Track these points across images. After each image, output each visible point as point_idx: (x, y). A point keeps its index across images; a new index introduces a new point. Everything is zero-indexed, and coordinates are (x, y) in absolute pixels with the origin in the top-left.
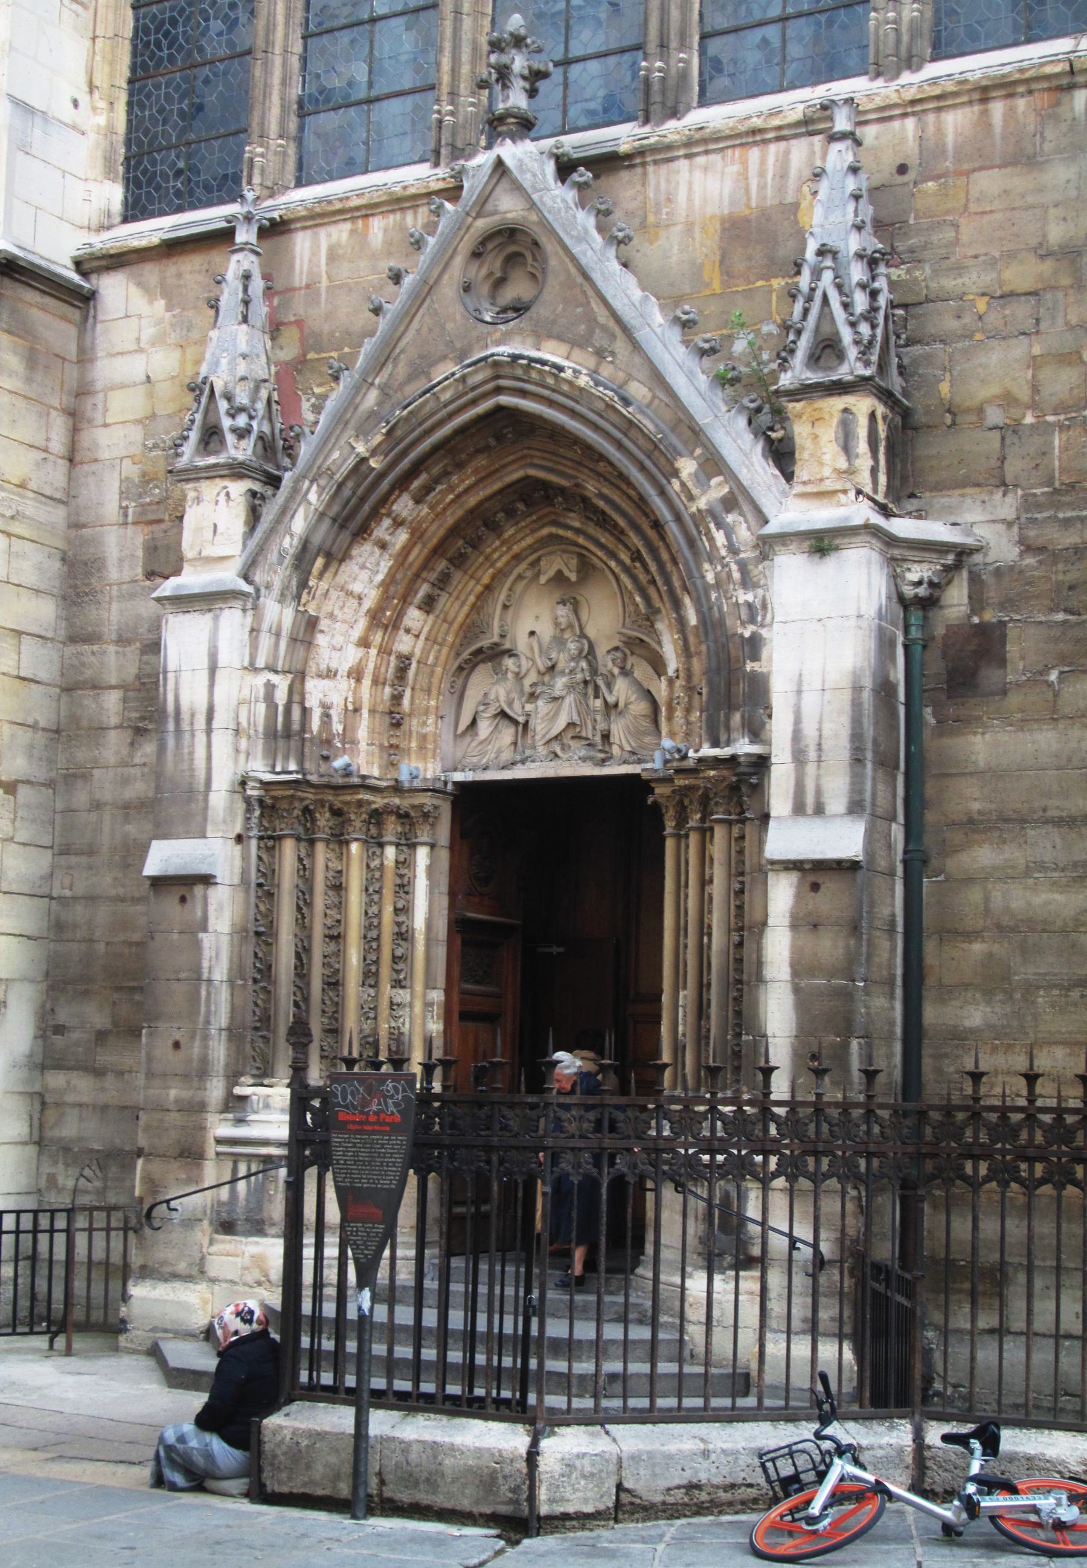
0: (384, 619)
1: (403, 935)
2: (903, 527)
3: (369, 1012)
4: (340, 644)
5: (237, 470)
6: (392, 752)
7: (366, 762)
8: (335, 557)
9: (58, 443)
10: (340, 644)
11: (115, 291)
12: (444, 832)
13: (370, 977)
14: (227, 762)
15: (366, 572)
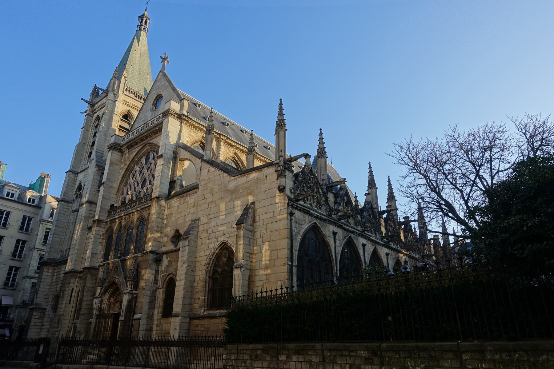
0: (109, 299)
1: (108, 327)
2: (133, 292)
3: (103, 334)
4: (105, 301)
5: (100, 286)
6: (109, 311)
7: (106, 312)
8: (105, 294)
9: (94, 282)
10: (105, 301)
11: (101, 268)
12: (112, 317)
13: (104, 331)
14: (95, 312)
15: (107, 295)
